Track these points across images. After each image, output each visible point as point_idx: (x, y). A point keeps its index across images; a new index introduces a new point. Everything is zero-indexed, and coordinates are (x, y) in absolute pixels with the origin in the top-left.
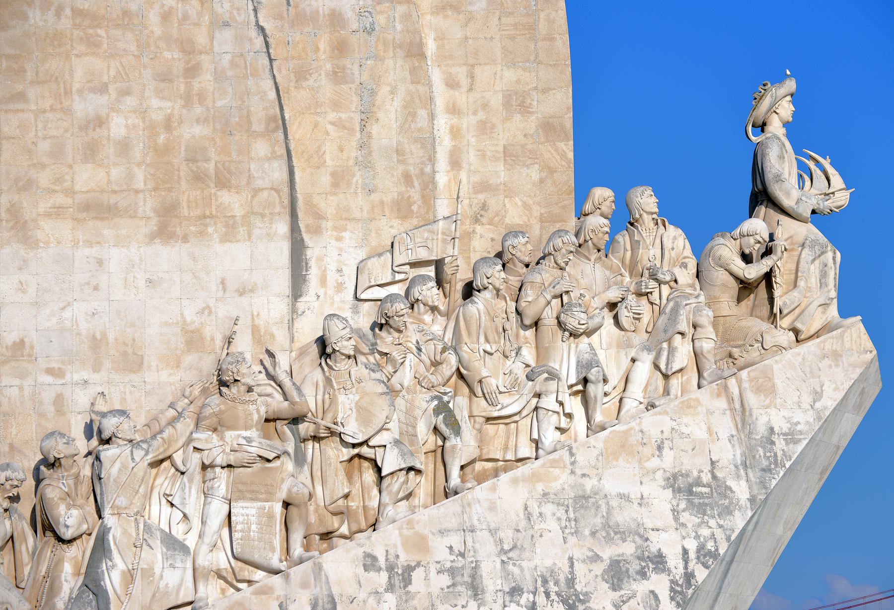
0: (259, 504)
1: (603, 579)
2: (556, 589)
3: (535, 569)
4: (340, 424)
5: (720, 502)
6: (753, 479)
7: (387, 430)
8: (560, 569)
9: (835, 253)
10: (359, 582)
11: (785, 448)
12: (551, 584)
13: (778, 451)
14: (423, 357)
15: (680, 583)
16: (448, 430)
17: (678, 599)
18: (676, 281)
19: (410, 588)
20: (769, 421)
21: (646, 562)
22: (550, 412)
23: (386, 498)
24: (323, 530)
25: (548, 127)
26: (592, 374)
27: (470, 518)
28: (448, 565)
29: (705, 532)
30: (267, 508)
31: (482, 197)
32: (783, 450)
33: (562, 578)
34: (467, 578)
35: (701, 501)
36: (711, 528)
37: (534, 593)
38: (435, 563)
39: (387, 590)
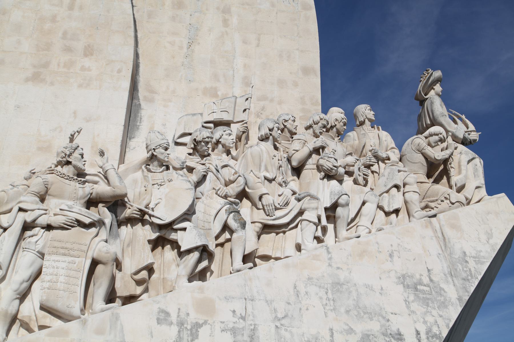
0: (72, 259)
3: (303, 335)
4: (151, 209)
5: (438, 299)
6: (458, 285)
7: (189, 220)
8: (323, 337)
9: (480, 160)
10: (151, 333)
11: (476, 267)
14: (219, 176)
16: (236, 224)
18: (389, 159)
20: (462, 248)
21: (389, 337)
22: (312, 224)
24: (126, 294)
25: (306, 71)
26: (343, 200)
28: (231, 325)
29: (430, 319)
30: (77, 263)
31: (262, 103)
32: (474, 268)
35: (424, 296)
36: (434, 316)
38: (220, 323)
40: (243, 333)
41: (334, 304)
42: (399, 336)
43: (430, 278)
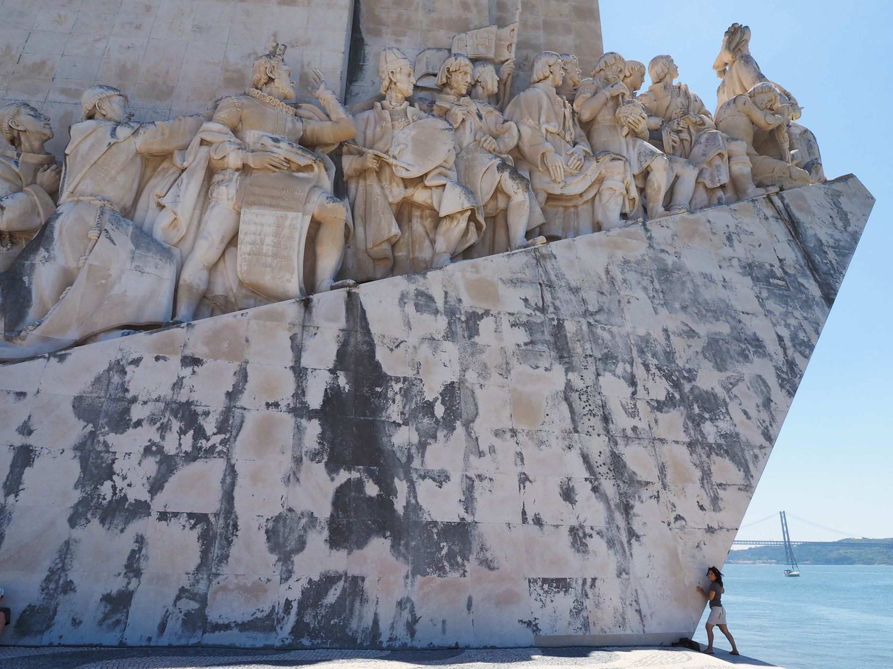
0: (280, 213)
1: (705, 357)
2: (655, 362)
5: (798, 296)
6: (819, 280)
10: (409, 322)
11: (837, 258)
12: (649, 355)
13: (832, 260)
15: (785, 369)
16: (515, 186)
17: (787, 387)
19: (476, 339)
21: (745, 344)
23: (441, 245)
27: (546, 272)
28: (524, 319)
33: (659, 349)
34: (547, 337)
35: (781, 292)
37: (632, 364)
39: (446, 338)
40: (542, 329)
41: (664, 297)
42: (757, 344)
43: (783, 269)
